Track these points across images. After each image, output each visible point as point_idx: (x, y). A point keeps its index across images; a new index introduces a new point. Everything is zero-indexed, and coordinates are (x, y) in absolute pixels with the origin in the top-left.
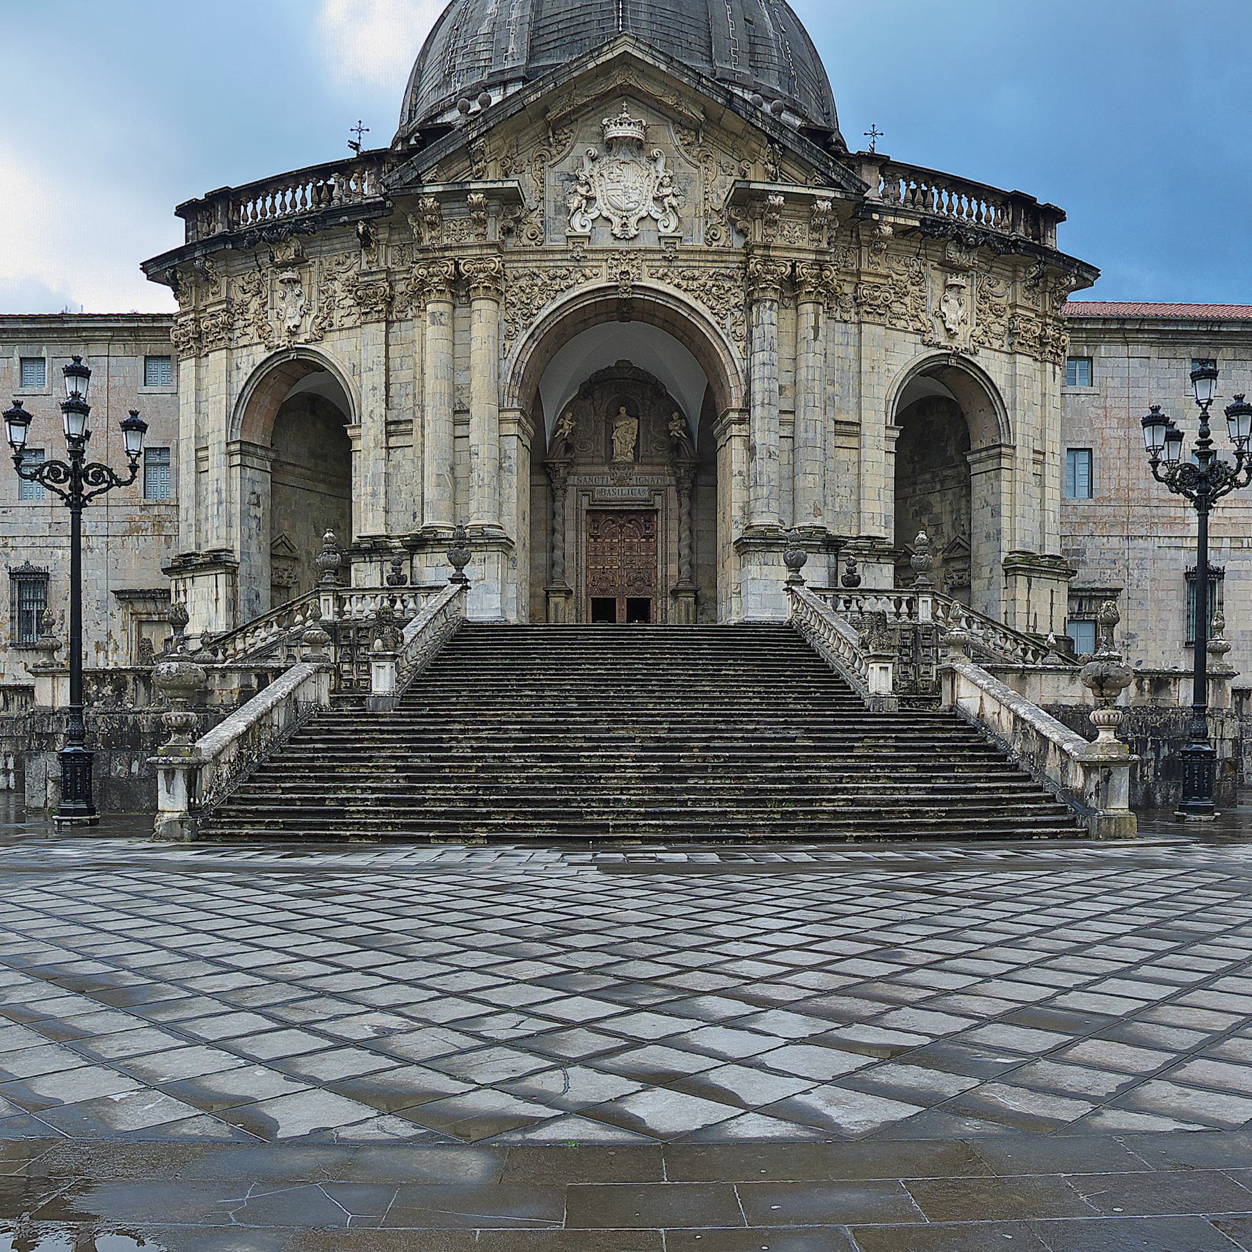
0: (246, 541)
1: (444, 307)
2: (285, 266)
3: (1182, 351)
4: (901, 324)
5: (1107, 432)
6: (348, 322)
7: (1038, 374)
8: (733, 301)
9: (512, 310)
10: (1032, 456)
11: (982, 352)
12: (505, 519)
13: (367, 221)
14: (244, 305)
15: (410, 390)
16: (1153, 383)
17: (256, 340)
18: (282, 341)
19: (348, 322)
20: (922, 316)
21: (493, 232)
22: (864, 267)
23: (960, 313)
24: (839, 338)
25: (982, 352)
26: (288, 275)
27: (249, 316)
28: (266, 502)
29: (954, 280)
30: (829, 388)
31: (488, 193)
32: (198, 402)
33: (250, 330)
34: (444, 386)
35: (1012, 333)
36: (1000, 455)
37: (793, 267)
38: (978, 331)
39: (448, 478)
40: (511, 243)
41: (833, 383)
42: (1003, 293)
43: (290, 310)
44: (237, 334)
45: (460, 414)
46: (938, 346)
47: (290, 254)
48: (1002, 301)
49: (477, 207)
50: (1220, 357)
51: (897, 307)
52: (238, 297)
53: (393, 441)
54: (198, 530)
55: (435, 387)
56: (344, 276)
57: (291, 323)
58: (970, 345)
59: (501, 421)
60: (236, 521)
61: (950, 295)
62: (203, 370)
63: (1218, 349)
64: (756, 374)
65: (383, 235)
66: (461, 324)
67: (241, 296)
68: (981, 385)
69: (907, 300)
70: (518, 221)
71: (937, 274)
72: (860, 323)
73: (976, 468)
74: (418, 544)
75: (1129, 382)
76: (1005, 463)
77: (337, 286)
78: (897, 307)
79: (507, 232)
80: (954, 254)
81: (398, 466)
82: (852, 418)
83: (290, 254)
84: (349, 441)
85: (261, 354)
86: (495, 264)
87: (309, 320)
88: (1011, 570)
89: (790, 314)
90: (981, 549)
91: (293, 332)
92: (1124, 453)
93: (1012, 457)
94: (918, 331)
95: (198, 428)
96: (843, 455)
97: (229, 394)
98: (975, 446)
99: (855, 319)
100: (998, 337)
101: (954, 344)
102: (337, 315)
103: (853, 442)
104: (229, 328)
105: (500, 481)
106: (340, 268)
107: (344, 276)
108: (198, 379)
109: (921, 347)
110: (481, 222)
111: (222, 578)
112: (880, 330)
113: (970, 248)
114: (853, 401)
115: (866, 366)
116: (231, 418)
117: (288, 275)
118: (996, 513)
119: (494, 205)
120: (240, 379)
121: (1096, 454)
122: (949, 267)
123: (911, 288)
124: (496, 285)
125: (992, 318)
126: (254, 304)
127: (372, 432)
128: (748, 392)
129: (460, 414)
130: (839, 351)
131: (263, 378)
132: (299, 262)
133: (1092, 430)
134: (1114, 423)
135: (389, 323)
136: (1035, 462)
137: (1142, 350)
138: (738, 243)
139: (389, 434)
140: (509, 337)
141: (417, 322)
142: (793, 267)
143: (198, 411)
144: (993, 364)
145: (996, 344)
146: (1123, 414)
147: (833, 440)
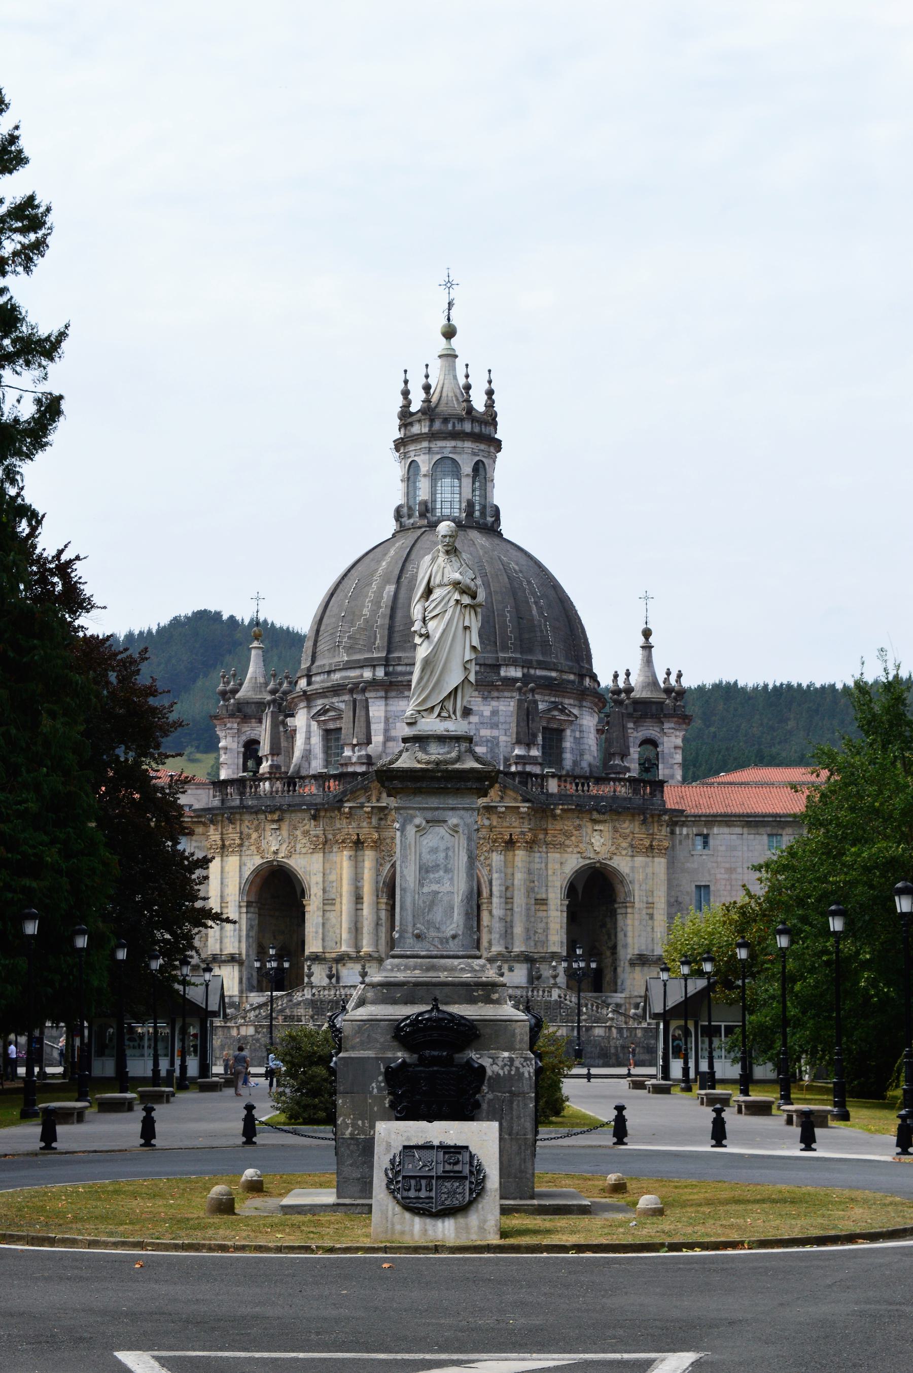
0: (247, 951)
1: (352, 853)
2: (273, 821)
3: (762, 830)
4: (571, 849)
5: (719, 876)
6: (304, 850)
7: (650, 864)
8: (485, 849)
9: (383, 853)
10: (645, 905)
11: (615, 857)
12: (380, 947)
13: (316, 810)
14: (249, 836)
15: (334, 884)
16: (745, 848)
17: (255, 853)
18: (270, 857)
19: (304, 850)
20: (581, 845)
21: (374, 821)
22: (550, 826)
23: (602, 840)
24: (537, 860)
25: (615, 857)
26: (274, 826)
27: (252, 841)
28: (256, 928)
29: (597, 828)
30: (532, 885)
31: (372, 807)
32: (222, 879)
33: (253, 848)
34: (353, 888)
35: (632, 846)
36: (626, 907)
37: (511, 835)
38: (613, 848)
39: (354, 931)
40: (383, 823)
41: (534, 882)
42: (627, 826)
43: (274, 843)
44: (245, 848)
45: (358, 899)
46: (590, 858)
47: (276, 817)
48: (627, 831)
49: (368, 813)
50: (784, 833)
51: (567, 842)
52: (246, 830)
53: (327, 908)
54: (221, 942)
55: (346, 888)
56: (302, 829)
57: (273, 848)
58: (608, 856)
59: (378, 903)
60: (244, 939)
61: (595, 833)
62: (224, 863)
63: (783, 828)
64: (494, 883)
65: (322, 814)
66: (360, 858)
67: (247, 830)
68: (615, 872)
69: (573, 838)
70: (386, 815)
71: (589, 824)
72: (547, 853)
73: (619, 911)
74: (341, 959)
75: (732, 848)
76: (629, 910)
77: (298, 833)
78: (567, 842)
79: (381, 819)
80: (595, 816)
81: (328, 919)
82: (544, 896)
83: (276, 817)
84: (304, 906)
85: (258, 861)
86: (376, 836)
87: (284, 846)
88: (632, 964)
89: (511, 853)
90: (621, 952)
91: (276, 853)
92: (728, 887)
93: (633, 907)
94: (579, 852)
95: (222, 892)
96: (540, 914)
97: (240, 877)
98: (618, 900)
99: (545, 850)
100: (625, 849)
101: (600, 857)
102: (299, 846)
103: (544, 908)
104: (241, 845)
105: (377, 932)
106: (300, 825)
107: (302, 829)
108: (222, 868)
109: (581, 860)
110: (370, 818)
111: (236, 968)
112: (558, 855)
113: (604, 814)
114: (544, 889)
115: (550, 872)
116: (241, 892)
117: (274, 826)
118: (625, 935)
119: (375, 811)
120: (247, 873)
121: (712, 888)
122: (595, 821)
123: (575, 832)
124: (377, 845)
125: (621, 840)
126: (254, 835)
127: (316, 903)
128: (491, 890)
129: (358, 899)
130: (537, 866)
131: (257, 872)
132: (280, 820)
133: (710, 875)
134: (723, 871)
135: (324, 853)
136: (647, 908)
137: (738, 830)
138: (487, 822)
139: (324, 904)
140: (381, 865)
141: (339, 854)
142: (511, 835)
143: (222, 883)
144: (622, 864)
145: (624, 852)
146: (727, 865)
147: (533, 908)
